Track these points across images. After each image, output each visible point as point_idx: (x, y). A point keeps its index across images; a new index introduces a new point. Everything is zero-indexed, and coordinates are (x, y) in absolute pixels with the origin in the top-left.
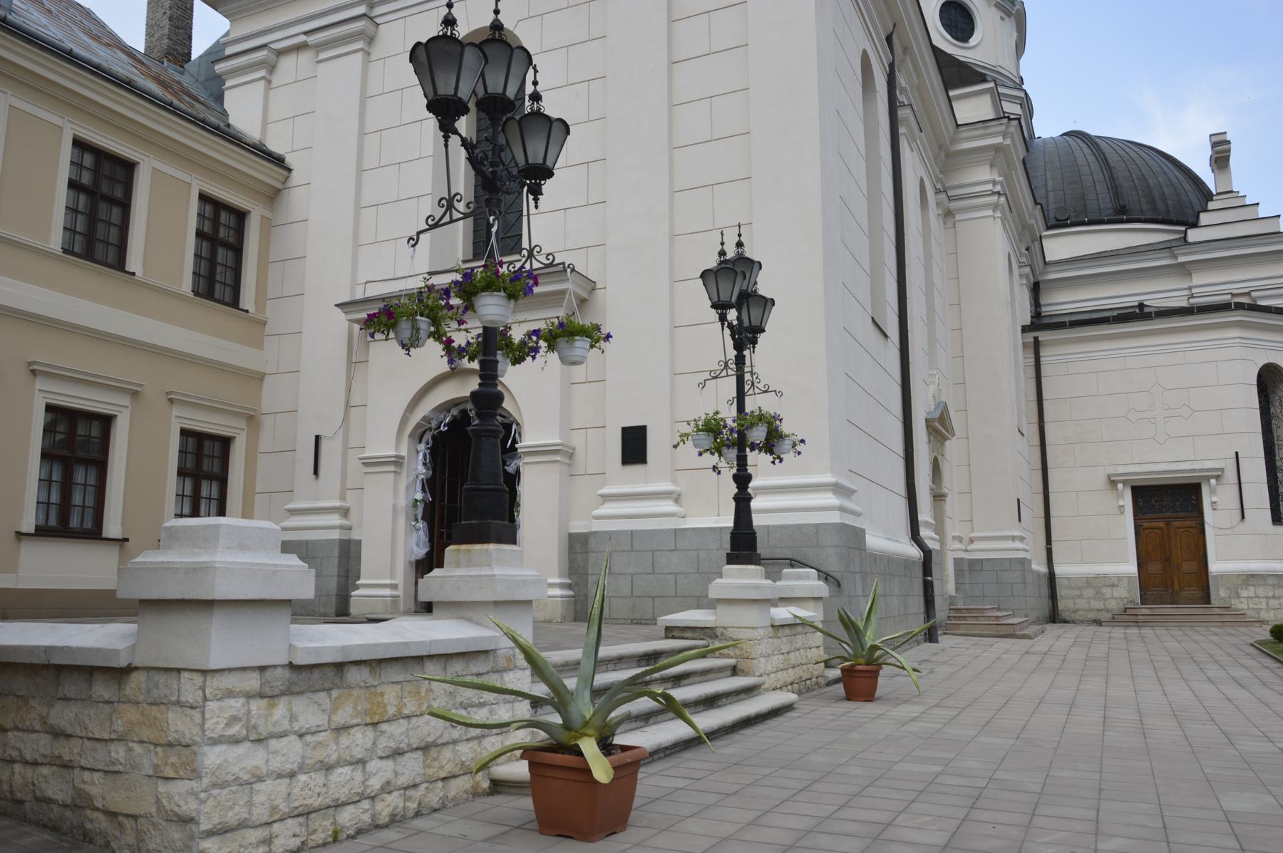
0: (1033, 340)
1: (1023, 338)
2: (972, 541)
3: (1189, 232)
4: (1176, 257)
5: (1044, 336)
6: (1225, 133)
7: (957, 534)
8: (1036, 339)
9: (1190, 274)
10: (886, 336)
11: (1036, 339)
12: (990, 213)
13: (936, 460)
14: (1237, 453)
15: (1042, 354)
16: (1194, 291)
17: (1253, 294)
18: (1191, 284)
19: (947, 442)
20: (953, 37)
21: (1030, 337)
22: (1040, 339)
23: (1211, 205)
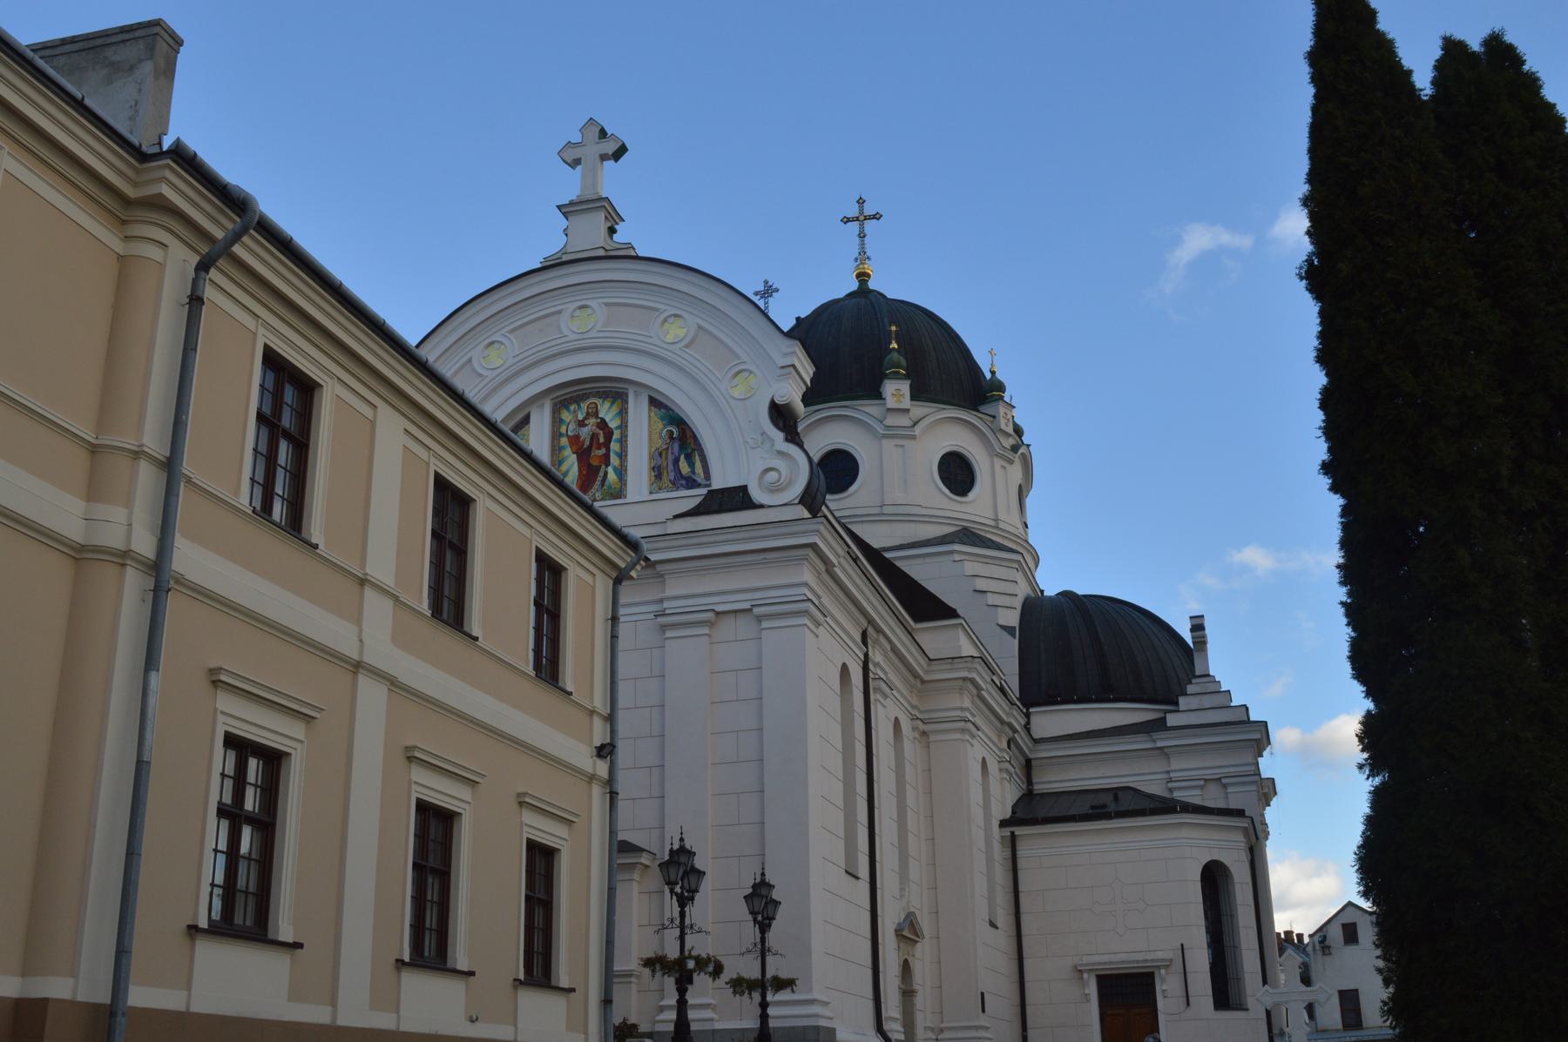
0: (1009, 834)
1: (1001, 832)
2: (942, 1031)
3: (1169, 716)
4: (1154, 741)
5: (1019, 831)
6: (1202, 616)
7: (930, 1025)
8: (1012, 833)
9: (1169, 758)
10: (857, 878)
11: (1012, 833)
12: (958, 736)
13: (906, 961)
14: (1182, 945)
15: (1018, 848)
16: (1172, 775)
17: (1224, 781)
18: (1169, 769)
19: (919, 945)
20: (951, 492)
21: (1007, 832)
22: (1016, 833)
23: (1190, 689)
